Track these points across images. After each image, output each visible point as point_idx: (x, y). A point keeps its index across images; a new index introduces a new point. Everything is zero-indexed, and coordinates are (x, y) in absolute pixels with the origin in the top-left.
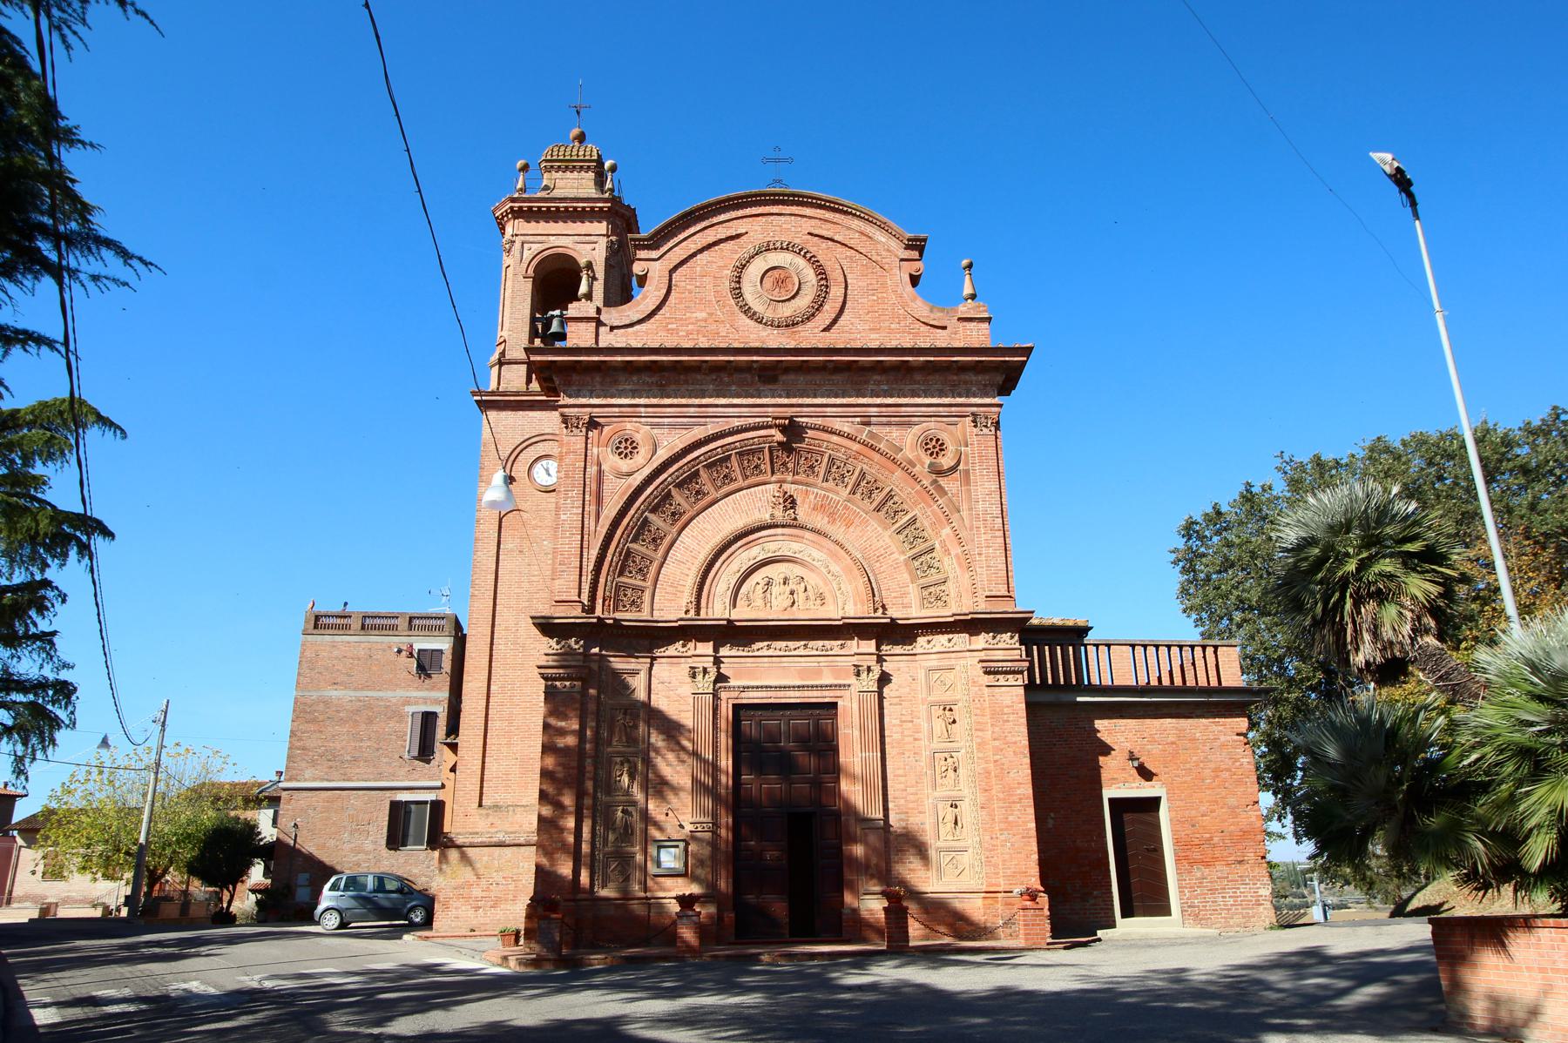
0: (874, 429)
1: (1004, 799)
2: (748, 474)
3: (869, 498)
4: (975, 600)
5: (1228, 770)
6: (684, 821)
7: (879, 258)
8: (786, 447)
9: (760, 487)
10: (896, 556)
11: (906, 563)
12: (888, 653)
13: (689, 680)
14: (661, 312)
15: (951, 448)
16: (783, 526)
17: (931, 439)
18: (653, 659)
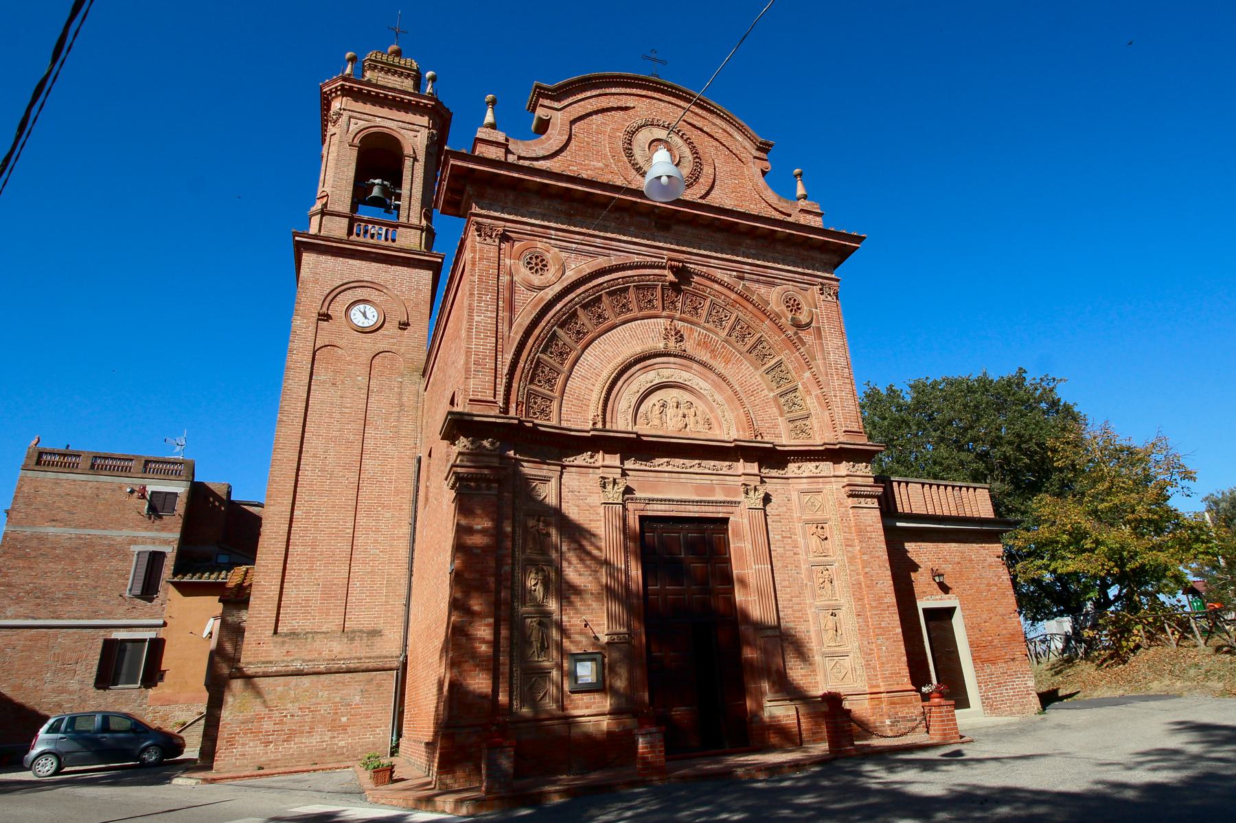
0: (747, 284)
1: (876, 607)
2: (642, 306)
3: (743, 341)
4: (836, 433)
5: (996, 585)
6: (599, 632)
7: (738, 152)
8: (676, 288)
9: (652, 320)
10: (766, 392)
11: (775, 399)
12: (767, 475)
14: (563, 154)
15: (805, 308)
16: (675, 356)
17: (790, 299)
18: (564, 467)
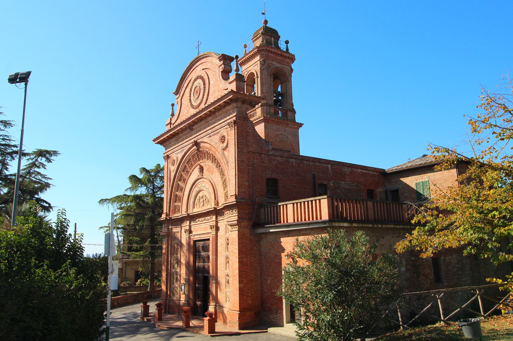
13: (185, 233)
18: (181, 227)
